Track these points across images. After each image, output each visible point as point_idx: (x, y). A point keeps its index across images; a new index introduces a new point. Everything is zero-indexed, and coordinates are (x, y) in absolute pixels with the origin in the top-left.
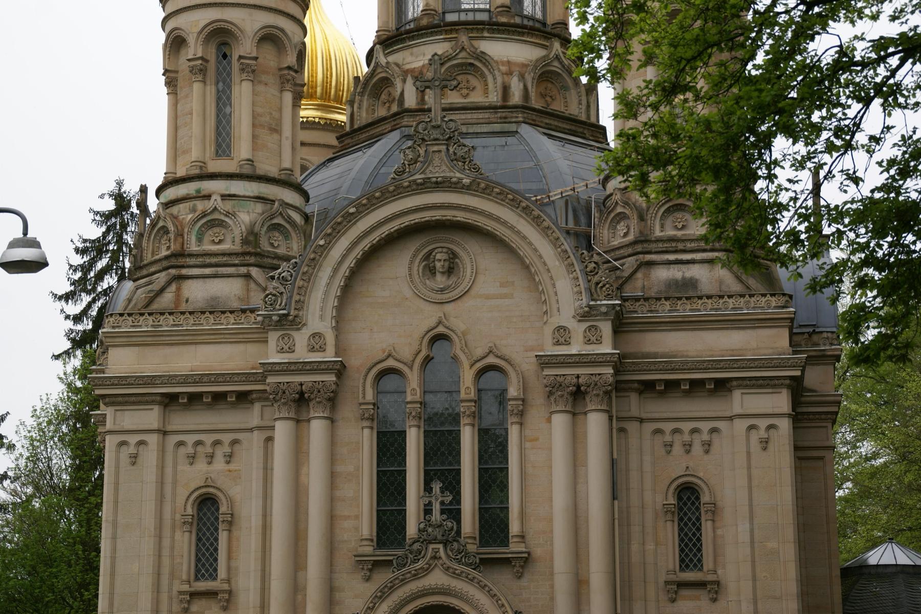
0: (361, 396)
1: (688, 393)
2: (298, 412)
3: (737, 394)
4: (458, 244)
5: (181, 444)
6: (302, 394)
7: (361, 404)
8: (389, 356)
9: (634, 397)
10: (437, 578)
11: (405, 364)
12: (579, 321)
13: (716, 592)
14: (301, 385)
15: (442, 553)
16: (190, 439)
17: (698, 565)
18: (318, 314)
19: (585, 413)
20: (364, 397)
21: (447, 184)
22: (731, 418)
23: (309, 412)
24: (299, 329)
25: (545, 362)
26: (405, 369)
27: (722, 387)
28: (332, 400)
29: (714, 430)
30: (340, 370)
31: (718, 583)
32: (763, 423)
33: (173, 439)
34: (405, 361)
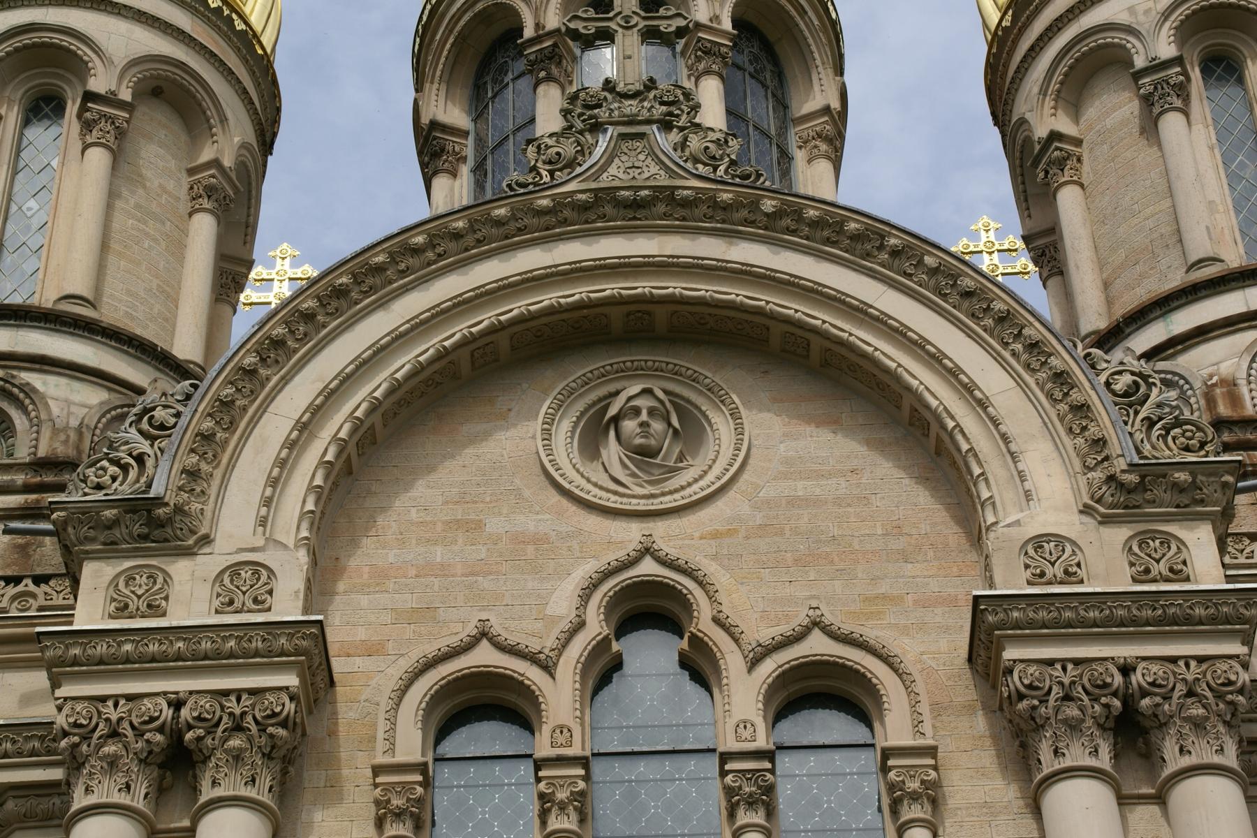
0: (381, 745)
2: (160, 793)
4: (694, 380)
6: (175, 734)
7: (377, 770)
8: (483, 634)
11: (532, 658)
12: (1106, 520)
14: (177, 704)
18: (254, 507)
19: (1160, 799)
20: (391, 750)
21: (661, 208)
23: (195, 790)
24: (189, 553)
26: (533, 674)
34: (534, 645)
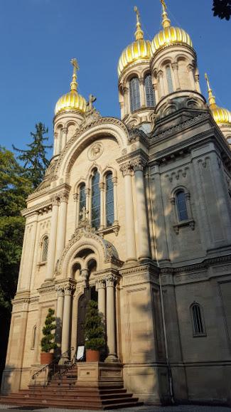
1: (174, 160)
3: (192, 152)
5: (41, 224)
9: (156, 167)
10: (83, 239)
13: (194, 226)
15: (84, 231)
16: (43, 222)
17: (187, 218)
22: (191, 162)
25: (119, 161)
27: (186, 152)
28: (66, 196)
29: (187, 168)
30: (67, 187)
31: (194, 222)
32: (203, 158)
33: (39, 223)
